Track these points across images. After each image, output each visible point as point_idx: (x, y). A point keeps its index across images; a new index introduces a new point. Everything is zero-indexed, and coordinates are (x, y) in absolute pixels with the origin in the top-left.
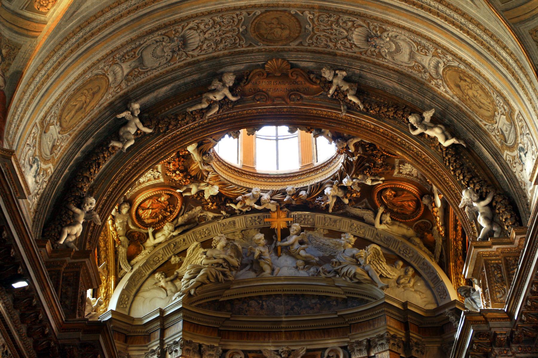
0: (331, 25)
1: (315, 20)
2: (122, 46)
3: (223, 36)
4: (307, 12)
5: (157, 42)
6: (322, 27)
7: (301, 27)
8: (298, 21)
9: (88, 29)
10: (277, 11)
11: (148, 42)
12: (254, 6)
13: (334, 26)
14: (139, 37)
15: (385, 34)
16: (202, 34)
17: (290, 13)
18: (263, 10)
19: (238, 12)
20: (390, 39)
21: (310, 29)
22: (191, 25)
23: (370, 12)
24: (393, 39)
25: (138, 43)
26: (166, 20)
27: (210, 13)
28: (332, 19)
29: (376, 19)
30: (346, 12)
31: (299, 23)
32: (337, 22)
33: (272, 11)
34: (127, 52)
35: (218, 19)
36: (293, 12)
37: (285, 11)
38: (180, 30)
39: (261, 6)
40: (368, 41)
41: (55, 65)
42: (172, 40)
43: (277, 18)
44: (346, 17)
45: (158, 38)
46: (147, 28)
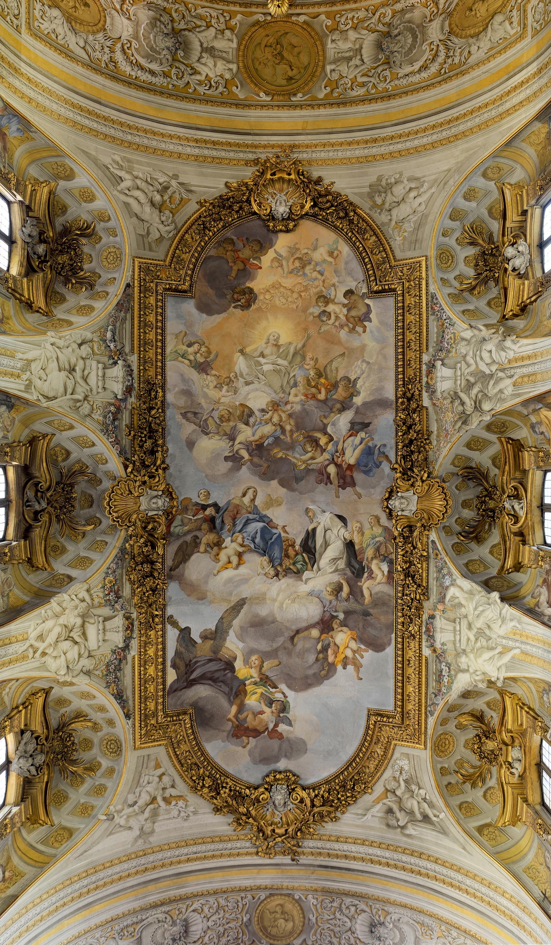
0: (334, 914)
1: (319, 906)
2: (124, 915)
3: (226, 927)
4: (310, 897)
5: (159, 921)
6: (327, 917)
7: (304, 917)
8: (302, 909)
9: (94, 878)
10: (281, 895)
11: (150, 920)
12: (259, 888)
13: (338, 915)
14: (143, 909)
15: (388, 918)
16: (205, 920)
17: (294, 899)
18: (268, 893)
19: (243, 895)
20: (394, 925)
21: (314, 920)
22: (195, 906)
23: (371, 891)
24: (396, 924)
25: (139, 917)
26: (172, 894)
27: (215, 893)
28: (335, 904)
29: (377, 900)
30: (347, 894)
31: (303, 913)
32: (341, 910)
33: (277, 895)
34: (127, 926)
35: (222, 902)
36: (297, 897)
37: (289, 895)
38: (184, 910)
39: (266, 888)
40: (372, 932)
41: (51, 909)
42: (174, 923)
43: (282, 905)
44: (348, 901)
45: (161, 916)
46: (152, 899)
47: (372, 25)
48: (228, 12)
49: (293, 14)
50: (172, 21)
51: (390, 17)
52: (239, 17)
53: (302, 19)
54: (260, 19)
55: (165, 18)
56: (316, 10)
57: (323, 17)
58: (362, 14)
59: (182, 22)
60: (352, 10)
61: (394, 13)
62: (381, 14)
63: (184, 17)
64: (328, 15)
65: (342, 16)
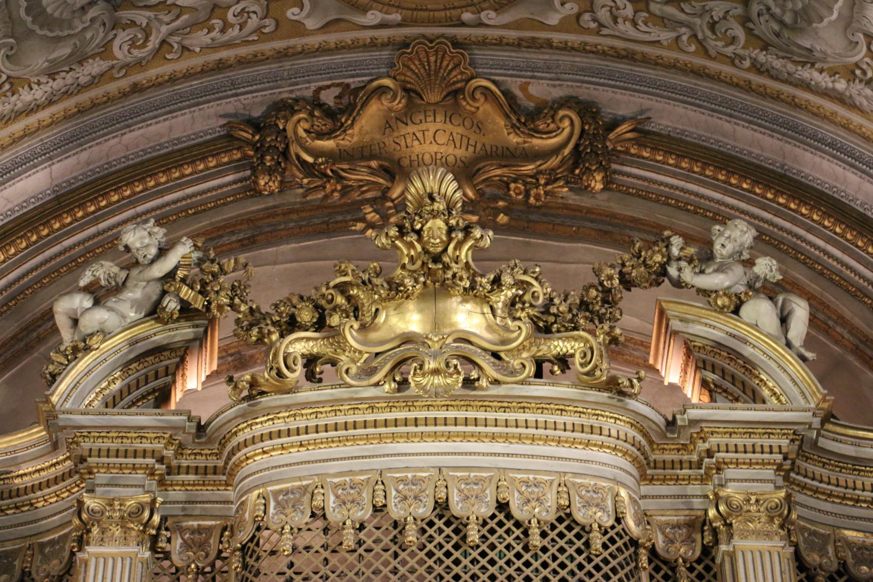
47: (167, 19)
48: (587, 31)
49: (399, 25)
50: (745, 21)
51: (116, 43)
52: (553, 19)
53: (373, 17)
54: (492, 14)
55: (765, 27)
56: (332, 38)
57: (311, 24)
58: (202, 38)
59: (717, 14)
60: (228, 45)
61: (105, 51)
62: (144, 45)
63: (712, 26)
64: (298, 28)
65: (258, 30)
